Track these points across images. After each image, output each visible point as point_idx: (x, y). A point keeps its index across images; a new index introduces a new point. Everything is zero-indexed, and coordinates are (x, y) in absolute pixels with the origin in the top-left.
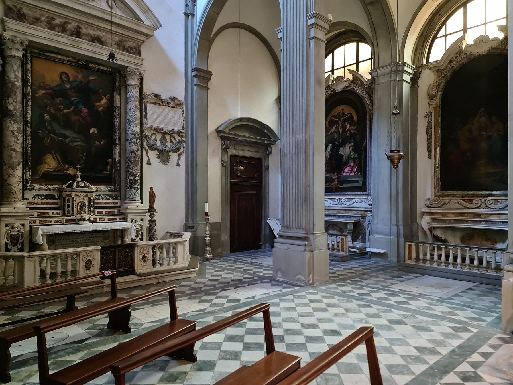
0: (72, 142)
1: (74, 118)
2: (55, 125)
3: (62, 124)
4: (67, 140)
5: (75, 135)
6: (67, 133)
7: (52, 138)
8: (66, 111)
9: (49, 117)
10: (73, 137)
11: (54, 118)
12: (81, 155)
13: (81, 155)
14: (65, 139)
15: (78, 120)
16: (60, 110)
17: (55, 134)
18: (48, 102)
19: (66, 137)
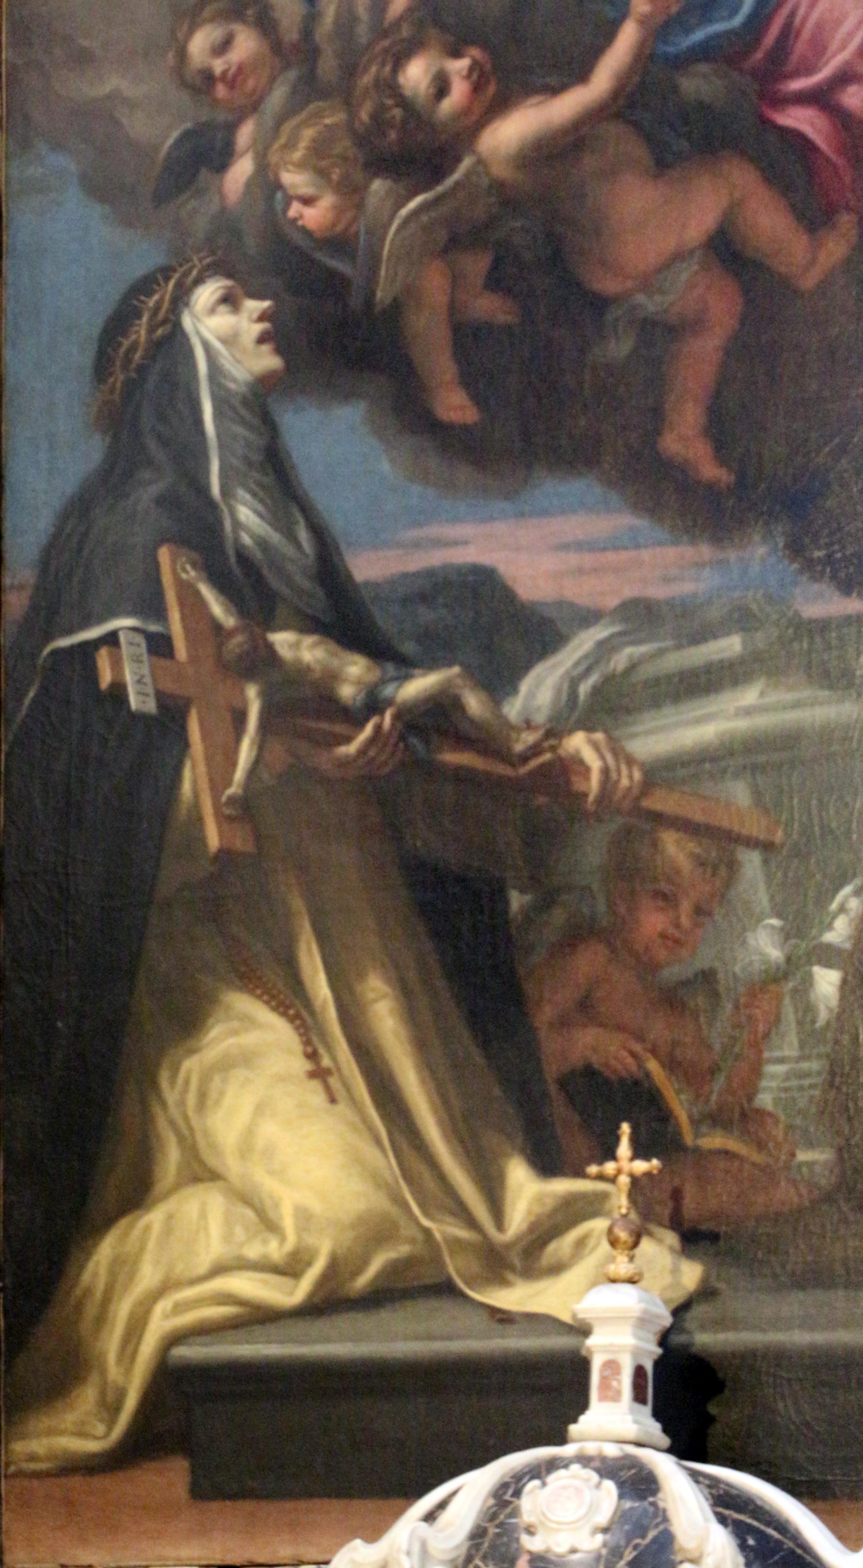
0: (609, 705)
1: (655, 227)
2: (339, 444)
3: (454, 405)
4: (539, 690)
5: (669, 566)
6: (554, 545)
7: (301, 707)
8: (511, 132)
9: (248, 320)
10: (641, 616)
11: (335, 330)
12: (766, 945)
13: (766, 945)
14: (499, 680)
15: (727, 250)
16: (415, 151)
17: (346, 618)
18: (246, 44)
19: (497, 628)
